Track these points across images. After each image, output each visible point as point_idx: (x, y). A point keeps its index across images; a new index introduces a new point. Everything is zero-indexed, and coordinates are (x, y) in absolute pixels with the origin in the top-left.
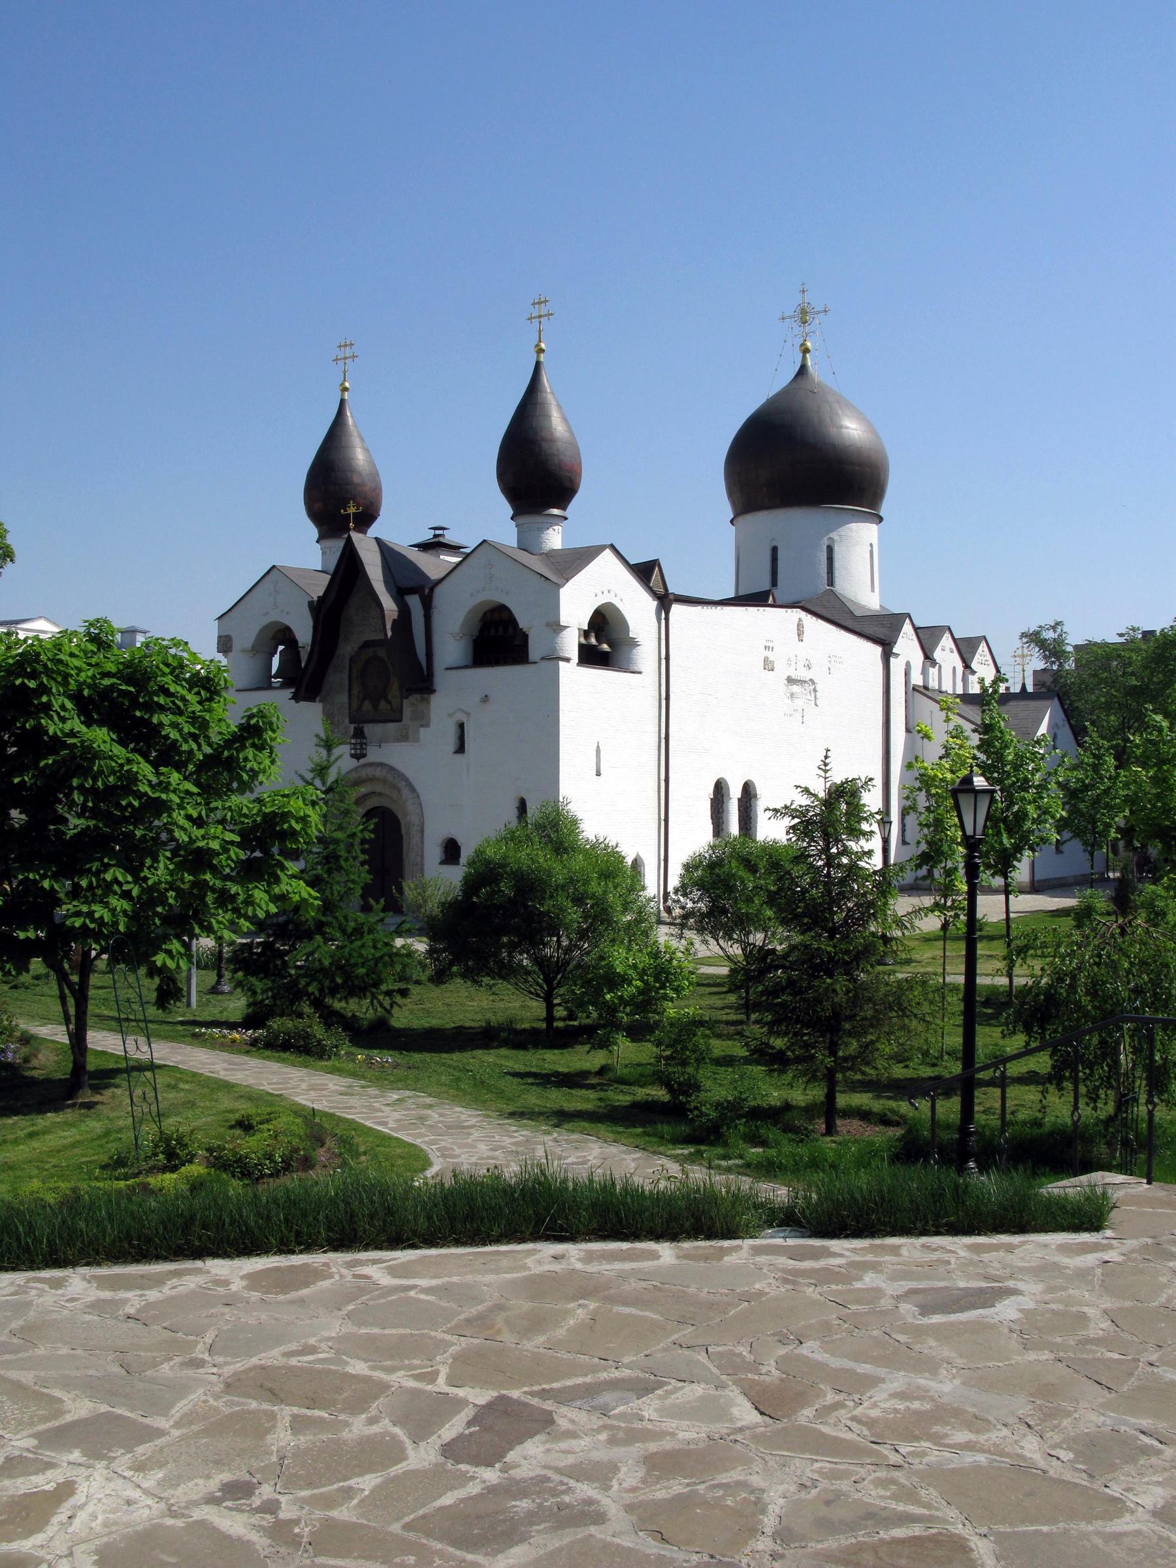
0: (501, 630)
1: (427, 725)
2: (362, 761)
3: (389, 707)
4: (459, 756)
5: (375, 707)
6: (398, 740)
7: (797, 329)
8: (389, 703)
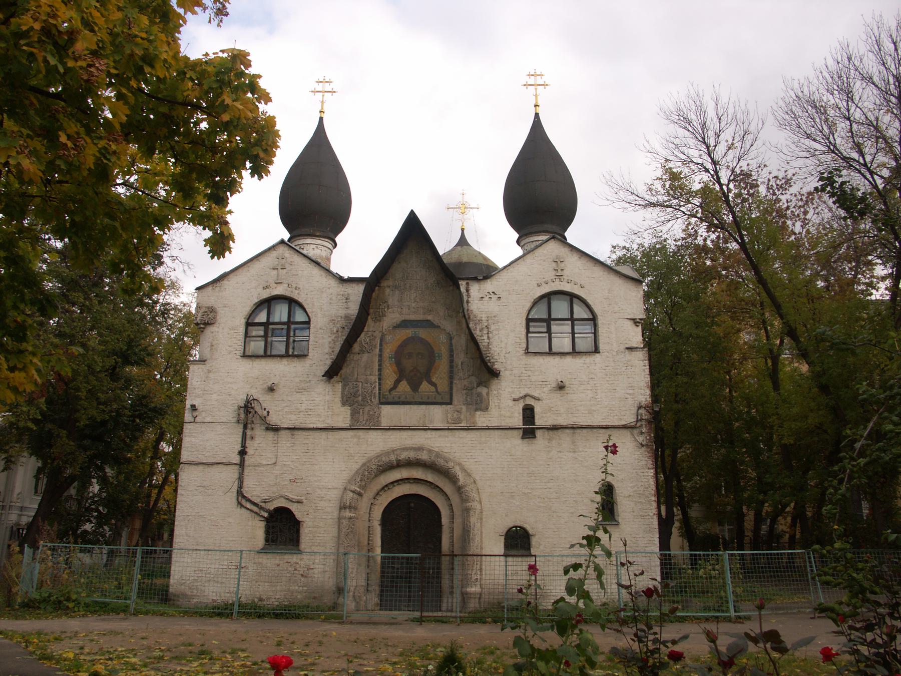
3: (433, 389)
5: (415, 387)
8: (434, 385)
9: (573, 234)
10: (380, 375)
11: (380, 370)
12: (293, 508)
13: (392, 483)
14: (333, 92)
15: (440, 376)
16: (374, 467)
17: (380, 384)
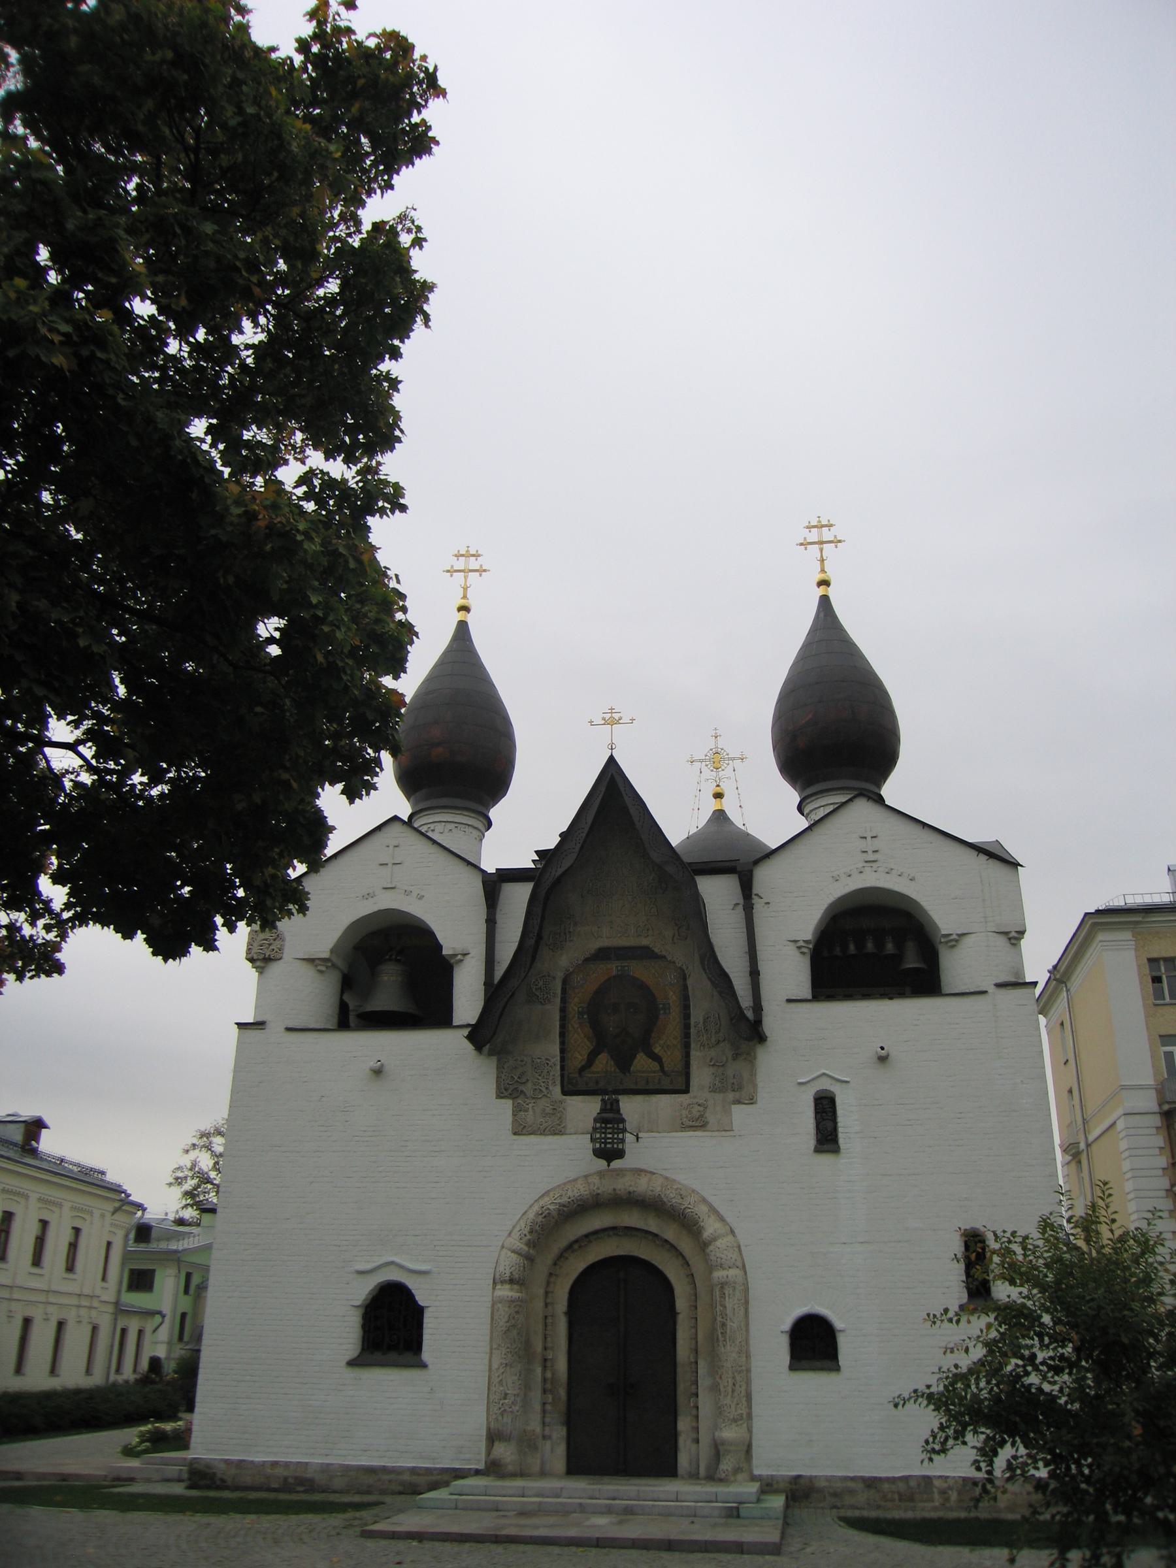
0: (870, 946)
1: (752, 1101)
2: (616, 1164)
3: (655, 1066)
4: (826, 1159)
5: (624, 1063)
6: (684, 1128)
7: (708, 773)
9: (893, 790)
10: (562, 1043)
11: (562, 1035)
12: (411, 1282)
13: (587, 1236)
14: (481, 571)
15: (666, 1042)
16: (552, 1207)
17: (562, 1059)
